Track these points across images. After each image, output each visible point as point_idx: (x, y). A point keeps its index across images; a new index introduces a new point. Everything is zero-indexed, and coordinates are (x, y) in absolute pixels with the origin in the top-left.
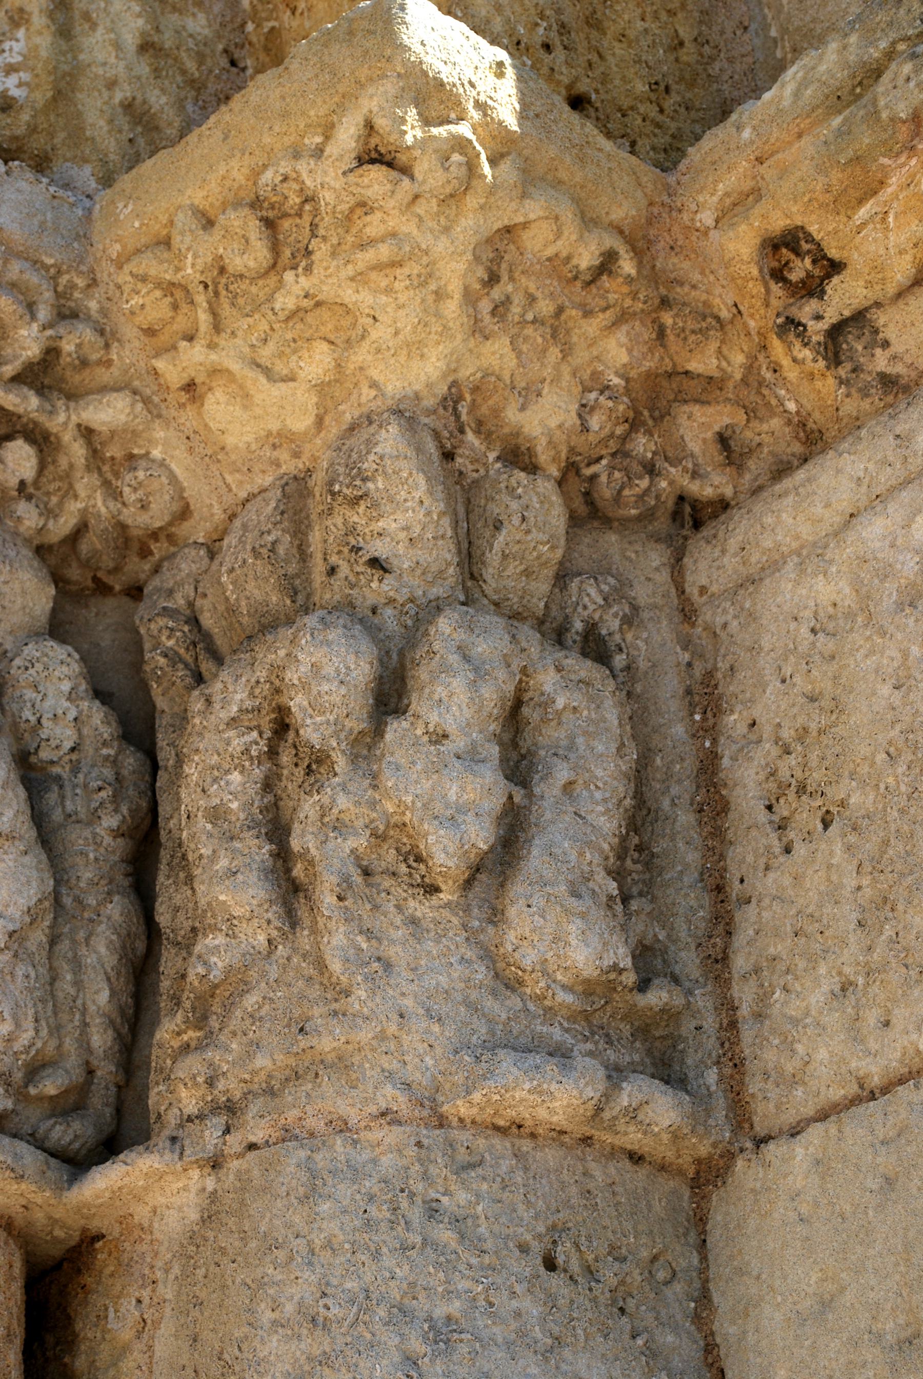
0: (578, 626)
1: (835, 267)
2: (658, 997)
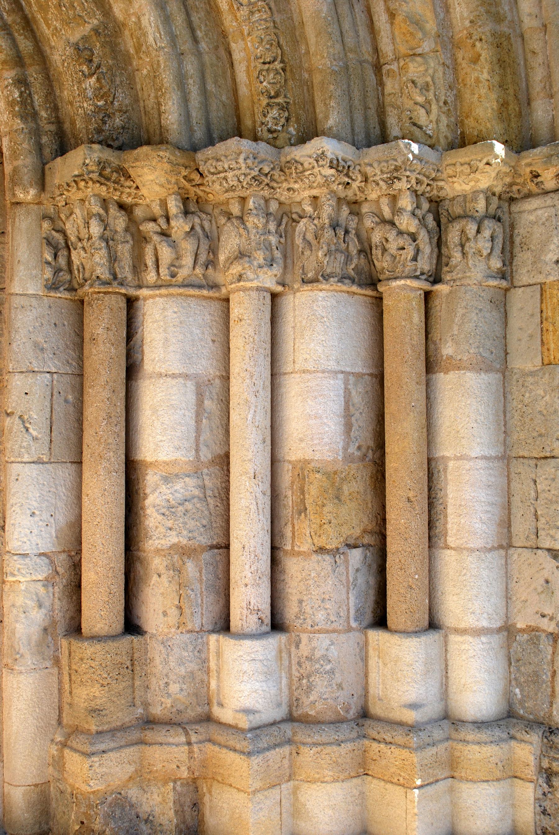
1: (539, 176)
2: (504, 268)
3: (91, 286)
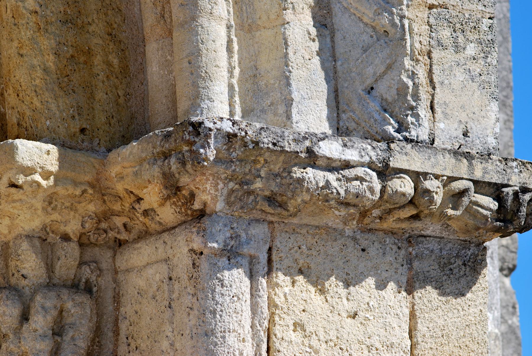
0: (84, 280)
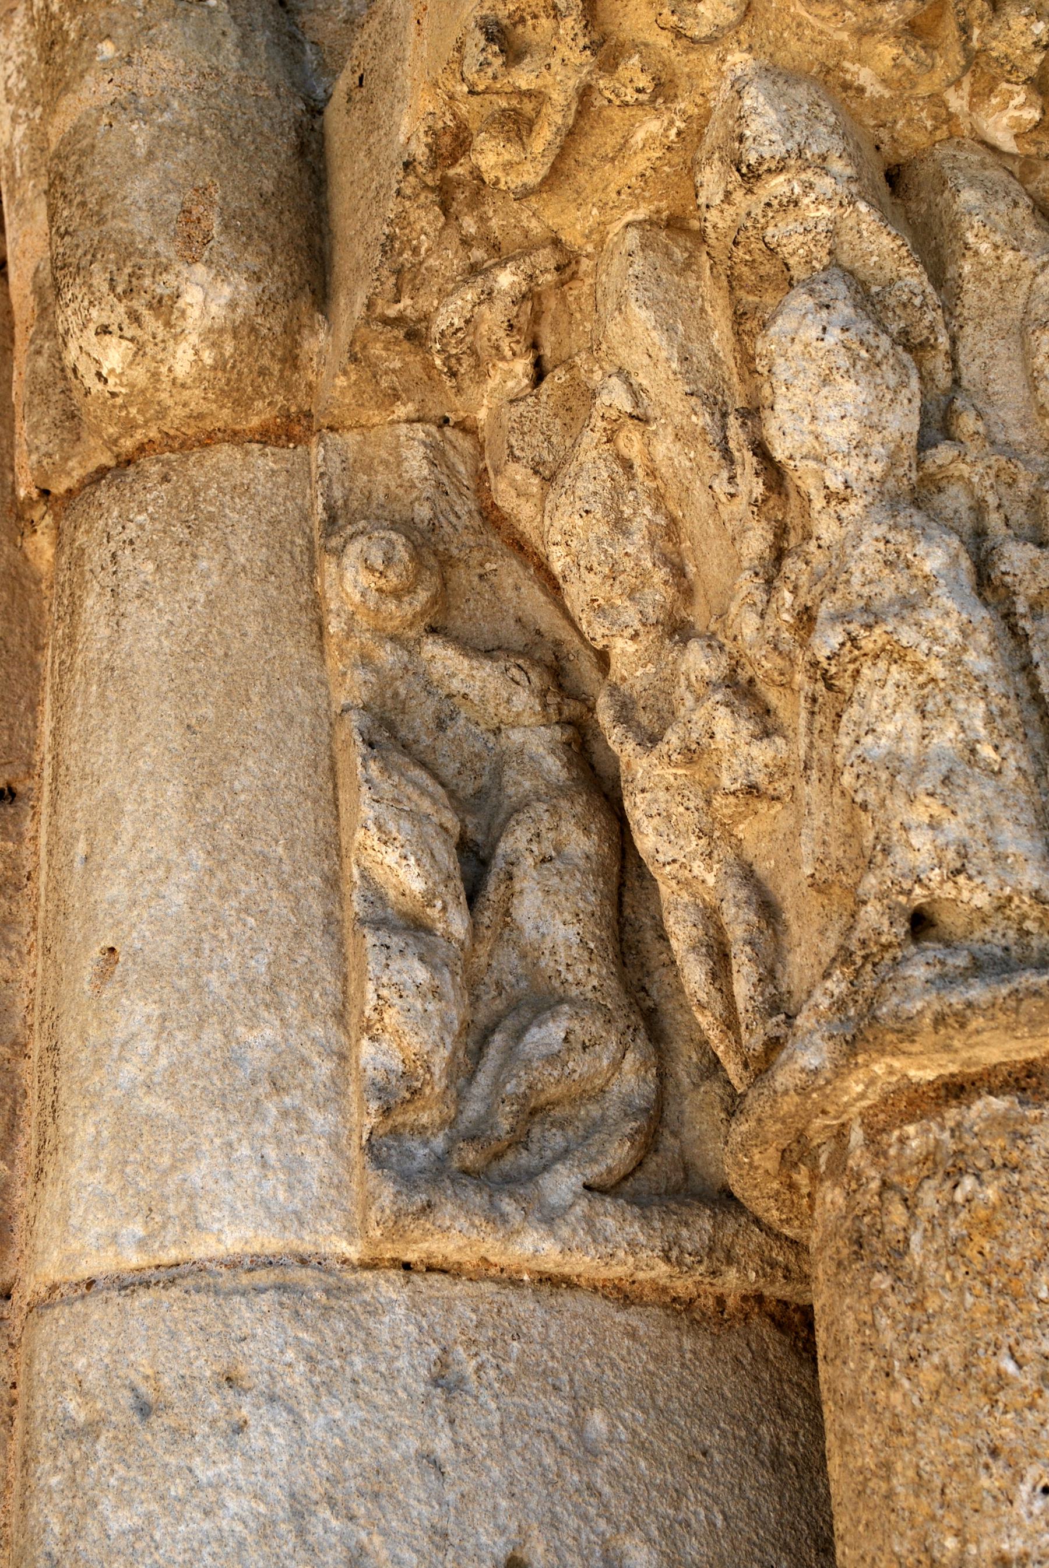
3: (860, 1032)
